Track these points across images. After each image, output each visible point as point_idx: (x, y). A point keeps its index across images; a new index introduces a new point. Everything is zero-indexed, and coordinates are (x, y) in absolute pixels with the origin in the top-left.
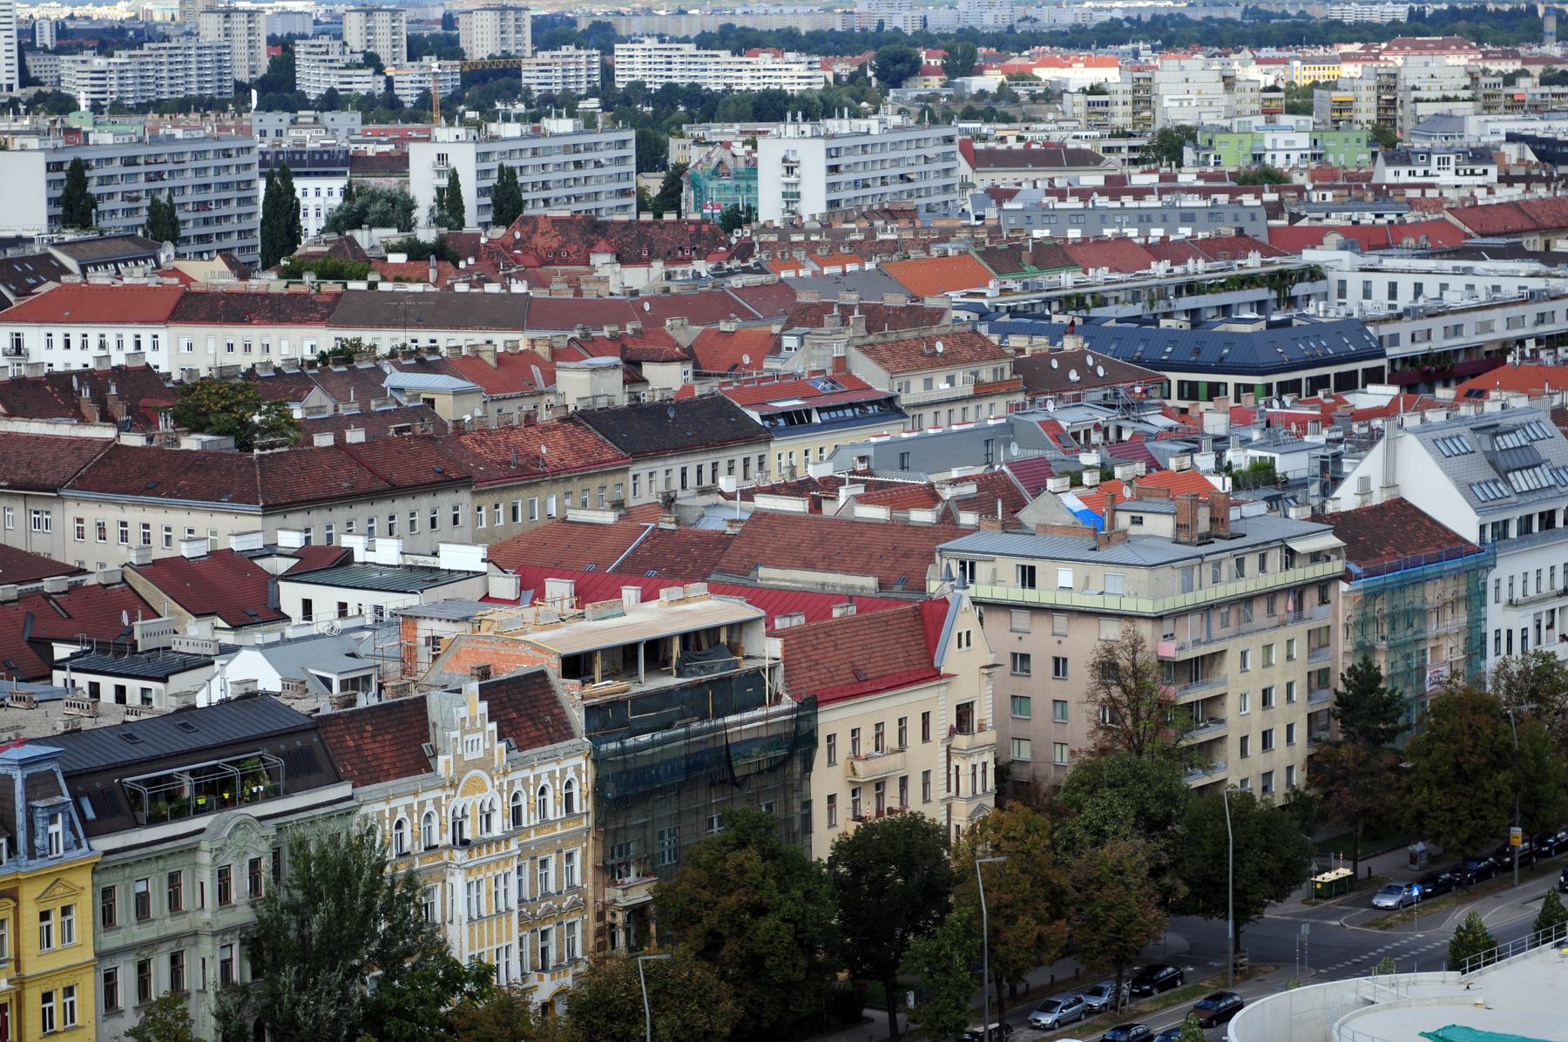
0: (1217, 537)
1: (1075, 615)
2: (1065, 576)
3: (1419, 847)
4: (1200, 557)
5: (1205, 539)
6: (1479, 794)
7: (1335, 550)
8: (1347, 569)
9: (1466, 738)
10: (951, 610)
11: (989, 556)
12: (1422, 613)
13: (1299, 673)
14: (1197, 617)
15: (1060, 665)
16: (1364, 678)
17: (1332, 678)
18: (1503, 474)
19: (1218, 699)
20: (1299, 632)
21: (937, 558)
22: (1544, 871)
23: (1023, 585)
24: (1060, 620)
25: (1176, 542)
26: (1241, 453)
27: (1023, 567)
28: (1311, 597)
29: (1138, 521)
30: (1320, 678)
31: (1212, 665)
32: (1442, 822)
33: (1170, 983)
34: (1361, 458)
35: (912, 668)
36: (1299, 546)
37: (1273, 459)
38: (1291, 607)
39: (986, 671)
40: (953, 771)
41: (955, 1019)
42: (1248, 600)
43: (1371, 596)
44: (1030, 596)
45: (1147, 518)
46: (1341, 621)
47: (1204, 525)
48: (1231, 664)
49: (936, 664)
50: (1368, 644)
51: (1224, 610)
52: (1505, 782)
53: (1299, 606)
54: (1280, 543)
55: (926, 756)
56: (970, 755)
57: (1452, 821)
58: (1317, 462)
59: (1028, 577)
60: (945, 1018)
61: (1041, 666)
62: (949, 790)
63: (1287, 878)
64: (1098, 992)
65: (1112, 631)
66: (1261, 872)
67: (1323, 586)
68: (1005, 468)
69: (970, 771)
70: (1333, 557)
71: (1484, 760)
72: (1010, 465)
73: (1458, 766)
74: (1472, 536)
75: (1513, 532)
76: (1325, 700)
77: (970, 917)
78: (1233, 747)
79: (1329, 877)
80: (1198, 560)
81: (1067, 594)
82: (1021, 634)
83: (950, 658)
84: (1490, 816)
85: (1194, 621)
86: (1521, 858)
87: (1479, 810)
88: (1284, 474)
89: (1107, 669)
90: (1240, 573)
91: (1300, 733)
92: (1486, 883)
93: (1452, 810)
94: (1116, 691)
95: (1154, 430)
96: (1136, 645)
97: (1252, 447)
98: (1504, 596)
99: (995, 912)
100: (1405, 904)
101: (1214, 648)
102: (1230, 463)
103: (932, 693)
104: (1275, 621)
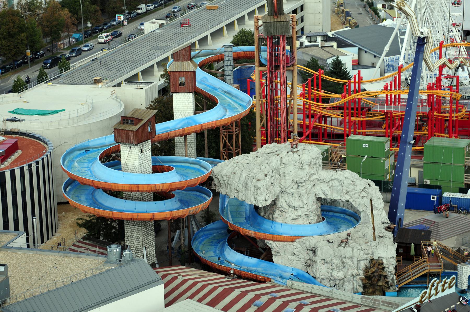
6: (16, 41)
9: (11, 24)
22: (37, 63)
32: (6, 50)
52: (24, 36)
57: (9, 49)
71: (17, 30)
73: (9, 32)
84: (20, 47)
86: (30, 59)
87: (17, 46)
92: (20, 68)
93: (8, 46)
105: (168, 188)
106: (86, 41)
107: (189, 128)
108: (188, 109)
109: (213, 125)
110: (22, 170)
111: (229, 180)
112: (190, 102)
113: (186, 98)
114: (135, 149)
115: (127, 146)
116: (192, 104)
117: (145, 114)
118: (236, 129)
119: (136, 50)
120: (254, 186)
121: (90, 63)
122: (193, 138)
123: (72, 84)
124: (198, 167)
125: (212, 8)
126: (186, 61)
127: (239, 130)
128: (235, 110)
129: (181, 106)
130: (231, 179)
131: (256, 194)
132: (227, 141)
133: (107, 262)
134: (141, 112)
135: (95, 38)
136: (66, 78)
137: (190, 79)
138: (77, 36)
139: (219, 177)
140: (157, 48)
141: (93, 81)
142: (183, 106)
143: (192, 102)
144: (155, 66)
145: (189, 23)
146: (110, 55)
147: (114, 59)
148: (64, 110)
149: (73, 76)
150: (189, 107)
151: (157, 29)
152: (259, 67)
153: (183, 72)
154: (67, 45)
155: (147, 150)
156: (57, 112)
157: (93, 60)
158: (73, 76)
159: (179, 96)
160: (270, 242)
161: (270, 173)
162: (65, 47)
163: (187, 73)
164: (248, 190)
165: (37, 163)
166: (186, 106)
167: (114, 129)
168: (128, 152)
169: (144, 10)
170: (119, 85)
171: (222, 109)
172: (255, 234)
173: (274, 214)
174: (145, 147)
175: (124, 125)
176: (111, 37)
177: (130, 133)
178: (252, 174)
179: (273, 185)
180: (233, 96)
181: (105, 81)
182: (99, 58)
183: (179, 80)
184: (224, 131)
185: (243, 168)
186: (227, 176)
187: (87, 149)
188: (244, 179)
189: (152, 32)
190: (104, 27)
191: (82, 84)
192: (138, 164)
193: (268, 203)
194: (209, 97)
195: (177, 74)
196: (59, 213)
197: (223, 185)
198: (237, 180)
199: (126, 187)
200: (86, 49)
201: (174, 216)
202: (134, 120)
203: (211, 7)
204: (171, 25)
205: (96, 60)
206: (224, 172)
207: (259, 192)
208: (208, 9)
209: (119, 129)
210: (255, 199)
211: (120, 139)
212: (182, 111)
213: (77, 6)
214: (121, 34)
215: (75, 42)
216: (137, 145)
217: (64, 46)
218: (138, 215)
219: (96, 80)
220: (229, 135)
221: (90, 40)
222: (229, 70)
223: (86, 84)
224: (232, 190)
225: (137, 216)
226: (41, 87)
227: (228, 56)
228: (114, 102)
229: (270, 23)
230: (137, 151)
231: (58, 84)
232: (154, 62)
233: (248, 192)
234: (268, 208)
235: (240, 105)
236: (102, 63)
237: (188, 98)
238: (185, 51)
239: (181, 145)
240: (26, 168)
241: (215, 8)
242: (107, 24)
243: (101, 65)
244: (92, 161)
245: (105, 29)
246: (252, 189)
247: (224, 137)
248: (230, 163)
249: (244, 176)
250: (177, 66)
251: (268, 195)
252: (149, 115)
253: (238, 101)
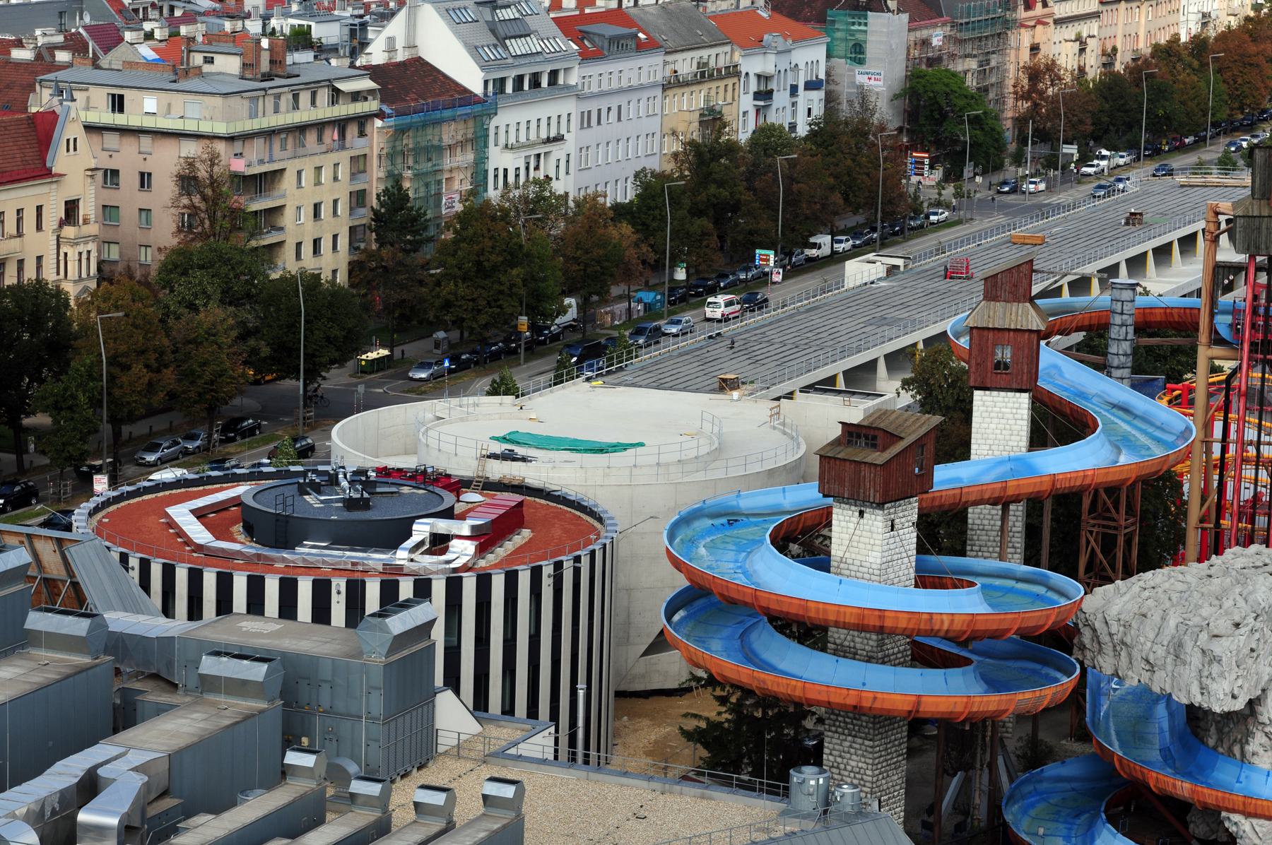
0: (276, 76)
1: (159, 136)
2: (150, 103)
3: (441, 335)
4: (264, 89)
5: (267, 77)
6: (496, 286)
7: (371, 92)
8: (381, 109)
9: (486, 240)
10: (61, 120)
11: (84, 85)
12: (439, 149)
13: (342, 192)
14: (262, 140)
15: (145, 179)
16: (395, 198)
17: (368, 199)
18: (501, 41)
19: (279, 210)
20: (343, 157)
21: (38, 87)
22: (542, 355)
23: (113, 111)
24: (146, 141)
25: (242, 78)
26: (283, 21)
27: (113, 96)
28: (352, 130)
29: (209, 61)
30: (358, 198)
31: (273, 181)
32: (465, 310)
33: (251, 432)
34: (383, 27)
35: (28, 167)
36: (344, 86)
37: (310, 27)
38: (336, 137)
39: (89, 173)
40: (62, 257)
41: (79, 449)
42: (302, 129)
43: (400, 131)
44: (120, 120)
45: (218, 59)
46: (376, 152)
47: (265, 66)
48: (288, 182)
49: (48, 165)
50: (396, 172)
51: (283, 136)
52: (518, 275)
53: (342, 135)
54: (328, 83)
55: (38, 244)
56: (77, 244)
57: (473, 309)
58: (346, 31)
59: (118, 104)
60: (71, 449)
61: (129, 180)
62: (58, 273)
63: (348, 347)
64: (192, 438)
65: (191, 149)
66: (328, 339)
67: (362, 121)
68: (81, 30)
69: (77, 257)
70: (370, 98)
71: (500, 259)
72: (85, 27)
73: (479, 264)
74: (478, 89)
75: (509, 88)
76: (364, 217)
77: (92, 363)
78: (289, 251)
79: (372, 355)
80: (262, 93)
81: (152, 118)
82: (111, 152)
83: (60, 160)
84: (505, 305)
85: (259, 143)
86: (526, 343)
87: (495, 301)
88: (320, 39)
89: (187, 181)
90: (296, 106)
91: (343, 242)
92: (498, 363)
93: (473, 300)
94: (197, 200)
95: (202, 10)
96: (213, 160)
97: (292, 17)
98: (502, 141)
99: (112, 361)
100: (434, 377)
101: (276, 167)
102: (274, 29)
103: (45, 189)
104: (324, 148)
105: (965, 628)
106: (671, 313)
107: (1021, 482)
108: (1013, 437)
109: (1087, 481)
110: (536, 574)
111: (1125, 634)
112: (1019, 417)
113: (1010, 405)
114: (873, 517)
115: (853, 508)
116: (1025, 423)
117: (908, 423)
118: (1126, 520)
119: (825, 323)
120: (1203, 652)
121: (703, 343)
122: (1020, 519)
123: (657, 388)
124: (1041, 590)
125: (1027, 241)
126: (1019, 302)
127: (1133, 524)
128: (1143, 452)
129: (993, 426)
130: (1132, 632)
131: (1205, 673)
132: (1098, 551)
133: (784, 813)
134: (897, 418)
135: (695, 309)
136: (641, 373)
137: (1026, 351)
138: (649, 297)
139: (1098, 625)
140: (883, 321)
141: (717, 385)
142: (999, 426)
143: (1026, 417)
144: (882, 367)
145: (967, 267)
146: (756, 329)
147: (766, 339)
148: (642, 445)
149: (660, 371)
150: (1015, 432)
151: (879, 279)
152: (1209, 346)
153: (1009, 330)
154: (620, 319)
155: (906, 525)
156: (624, 447)
157: (710, 337)
158: (660, 371)
159: (990, 399)
160: (1236, 817)
161: (1250, 620)
162: (616, 323)
163: (1019, 334)
164: (1184, 663)
165: (577, 559)
166: (1008, 427)
167: (821, 456)
168: (852, 526)
169: (826, 251)
170: (790, 396)
171: (1108, 447)
172: (1193, 792)
173: (1247, 742)
174: (901, 515)
175: (849, 450)
176: (739, 306)
177: (865, 471)
178: (1196, 620)
179: (1255, 654)
180: (1136, 416)
181: (749, 387)
182: (727, 334)
183: (994, 354)
184: (1092, 522)
185: (1168, 604)
186: (1122, 623)
187: (732, 517)
188: (1174, 631)
189: (866, 284)
190: (719, 282)
191: (684, 389)
192: (879, 561)
193: (1239, 705)
194: (1068, 412)
195: (991, 335)
196: (617, 717)
197: (1108, 649)
198: (1151, 635)
199: (848, 615)
200: (674, 330)
201: (975, 709)
202: (880, 435)
203: (1024, 237)
204: (918, 273)
205: (719, 339)
206: (1113, 612)
207: (1215, 669)
208: (1015, 244)
209: (836, 459)
210: (1202, 688)
211: (836, 488)
212: (997, 442)
213: (654, 219)
214: (766, 300)
215: (641, 314)
216: (880, 506)
217: (613, 319)
218: (875, 698)
219: (724, 380)
220: (1105, 534)
221: (683, 310)
222: (1121, 352)
223: (697, 391)
224: (1135, 663)
225: (871, 700)
226: (573, 389)
227: (1122, 313)
228: (777, 434)
229: (1257, 219)
230: (880, 524)
231: (619, 384)
232: (878, 352)
233: (1182, 667)
234: (1232, 726)
235: (1158, 440)
236: (736, 345)
237: (1016, 405)
238: (1019, 272)
239: (984, 538)
240: (548, 570)
241: (1034, 242)
242: (727, 276)
243: (733, 350)
244: (750, 546)
245: (721, 289)
246: (1195, 659)
247: (1092, 540)
248: (1129, 589)
249: (1172, 622)
250: (991, 314)
251: (1240, 682)
252: (920, 427)
253: (1150, 430)
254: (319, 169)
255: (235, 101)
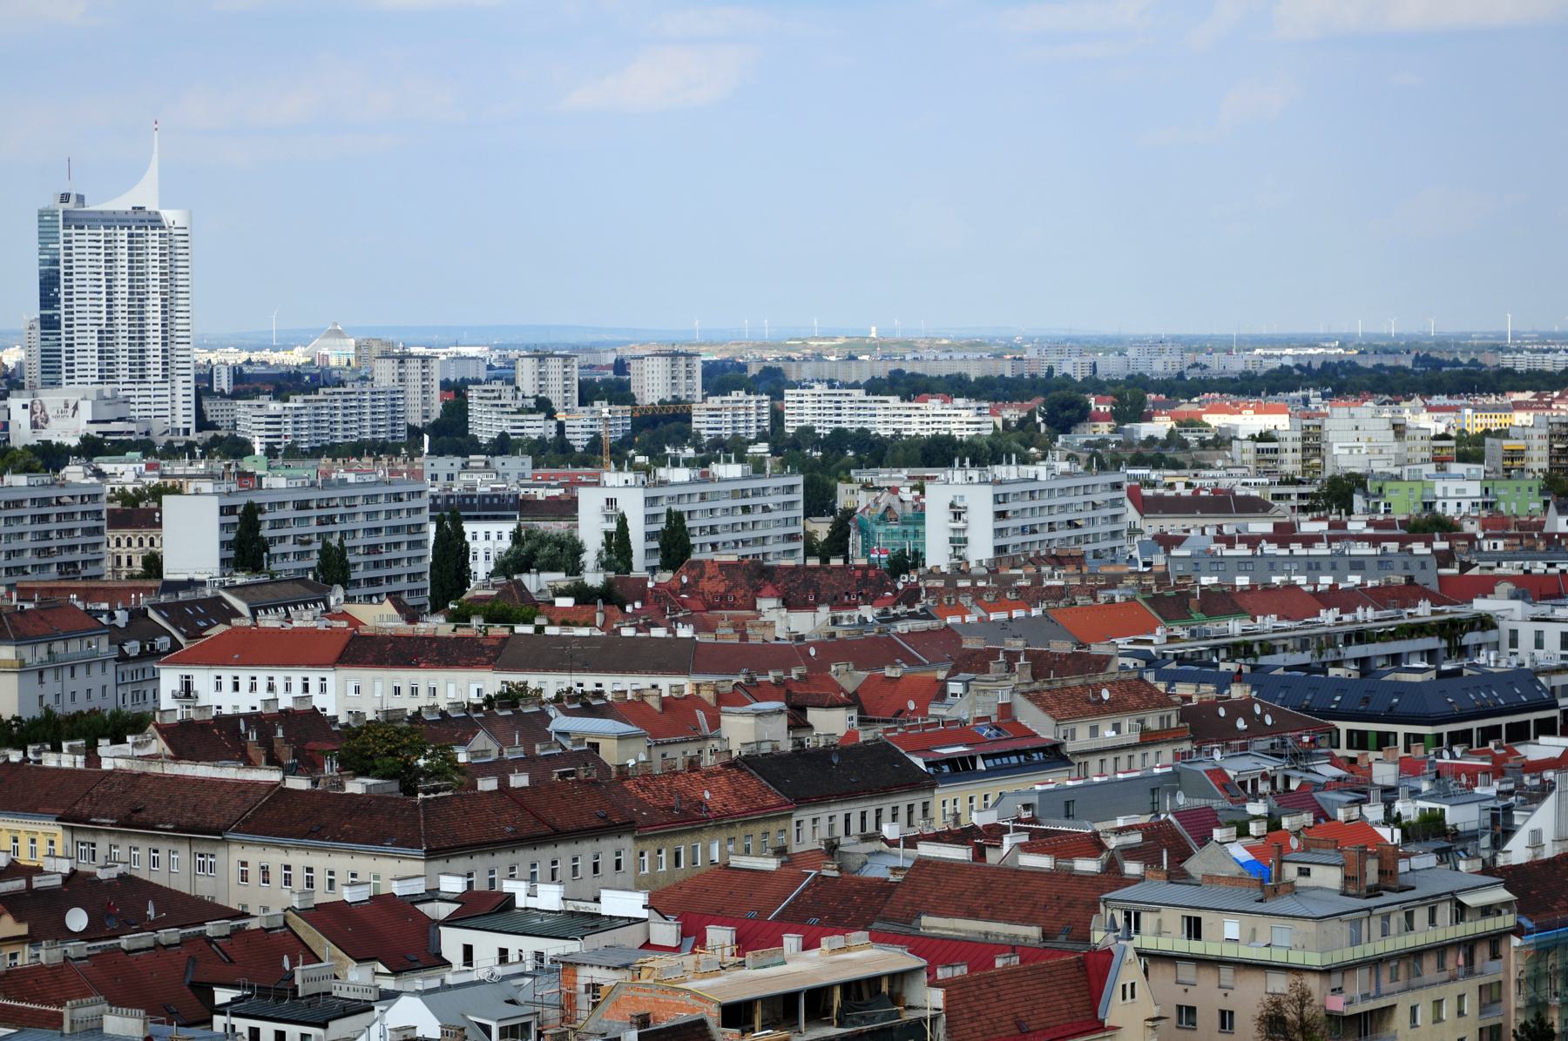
0: (1387, 889)
1: (1242, 968)
2: (1232, 928)
4: (1369, 909)
5: (1374, 892)
7: (1506, 904)
8: (1519, 924)
10: (1115, 961)
11: (1155, 906)
17: (1504, 1034)
20: (1470, 987)
21: (1102, 908)
23: (1189, 937)
24: (1227, 973)
25: (1344, 893)
26: (1410, 804)
27: (1189, 918)
28: (1482, 952)
29: (1305, 873)
31: (1381, 1020)
34: (1532, 811)
36: (1469, 900)
37: (1443, 811)
38: (1461, 961)
39: (1150, 1024)
42: (1417, 954)
43: (1542, 951)
44: (1196, 947)
45: (1315, 870)
46: (1513, 976)
47: (1372, 877)
48: (1401, 1018)
49: (1100, 1016)
50: (1540, 1000)
51: (1394, 964)
53: (1470, 961)
54: (1449, 896)
58: (1488, 814)
59: (1194, 929)
65: (1279, 984)
67: (1494, 941)
68: (1170, 817)
70: (1504, 911)
72: (1176, 814)
80: (1366, 913)
81: (1233, 946)
82: (1187, 986)
85: (1362, 975)
88: (1455, 826)
90: (1410, 926)
95: (1323, 780)
96: (1304, 998)
97: (1422, 799)
101: (1383, 1003)
102: (1399, 814)
104: (1445, 975)
254: (1438, 1003)
255: (1332, 925)
